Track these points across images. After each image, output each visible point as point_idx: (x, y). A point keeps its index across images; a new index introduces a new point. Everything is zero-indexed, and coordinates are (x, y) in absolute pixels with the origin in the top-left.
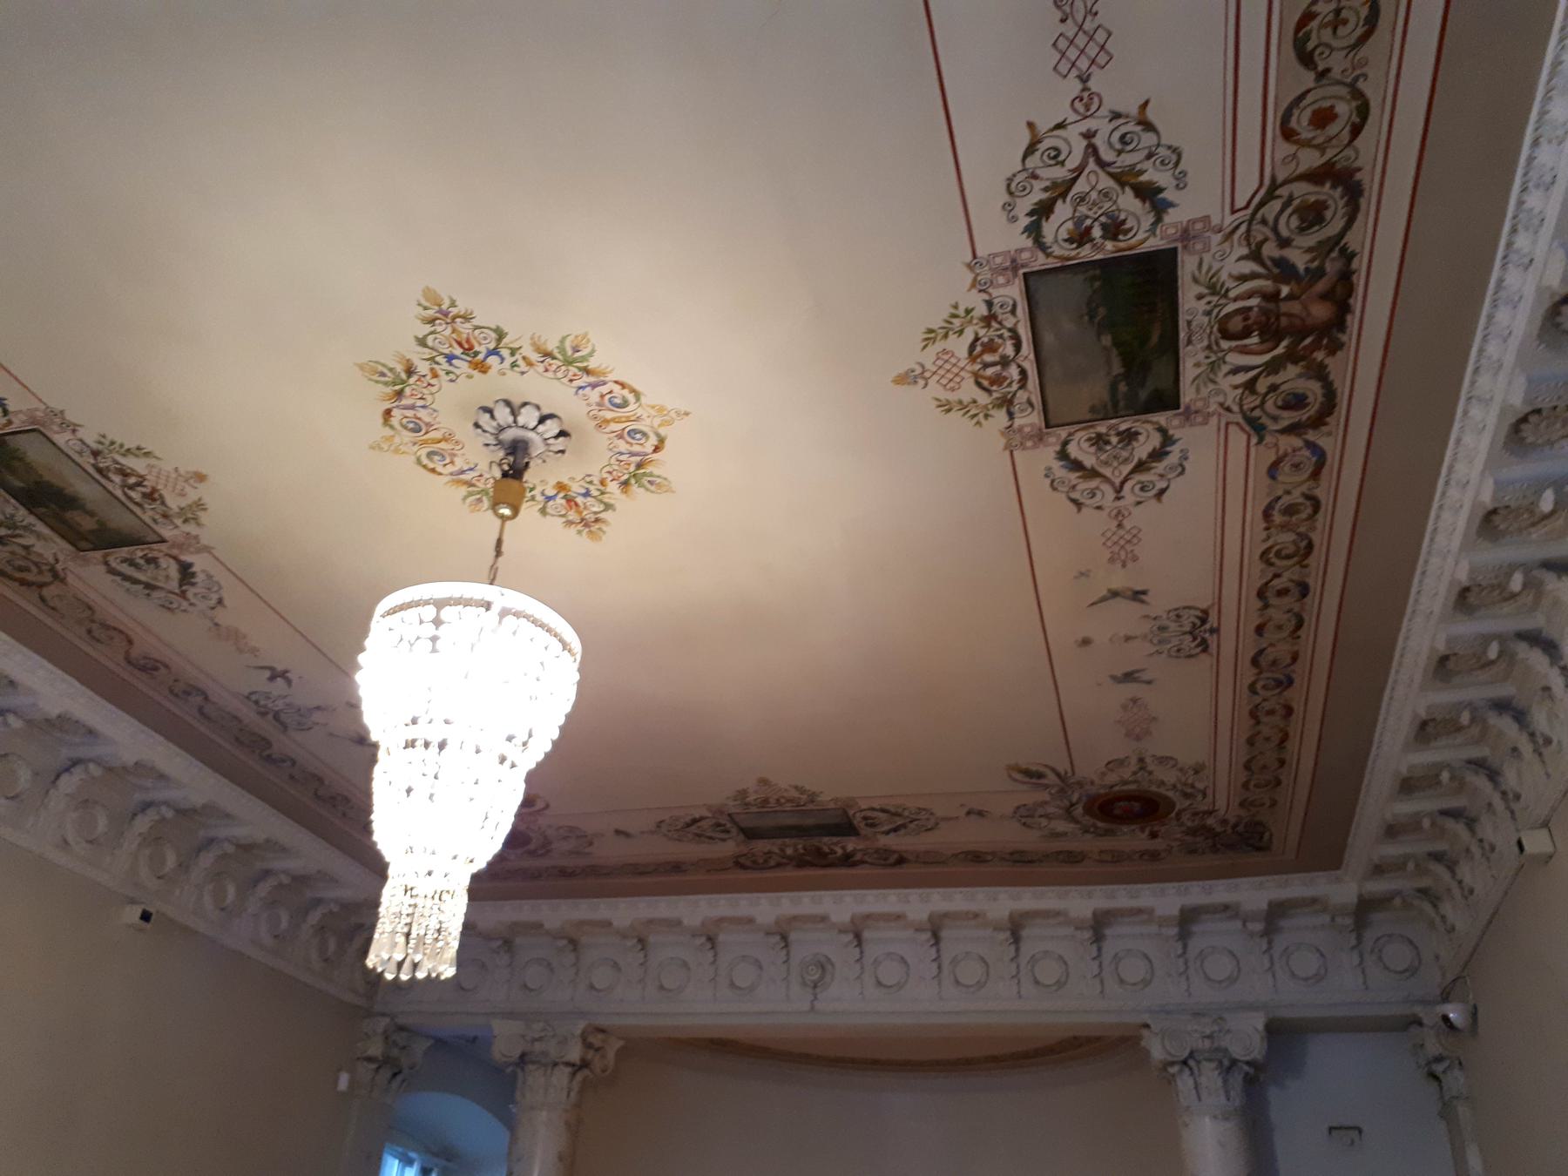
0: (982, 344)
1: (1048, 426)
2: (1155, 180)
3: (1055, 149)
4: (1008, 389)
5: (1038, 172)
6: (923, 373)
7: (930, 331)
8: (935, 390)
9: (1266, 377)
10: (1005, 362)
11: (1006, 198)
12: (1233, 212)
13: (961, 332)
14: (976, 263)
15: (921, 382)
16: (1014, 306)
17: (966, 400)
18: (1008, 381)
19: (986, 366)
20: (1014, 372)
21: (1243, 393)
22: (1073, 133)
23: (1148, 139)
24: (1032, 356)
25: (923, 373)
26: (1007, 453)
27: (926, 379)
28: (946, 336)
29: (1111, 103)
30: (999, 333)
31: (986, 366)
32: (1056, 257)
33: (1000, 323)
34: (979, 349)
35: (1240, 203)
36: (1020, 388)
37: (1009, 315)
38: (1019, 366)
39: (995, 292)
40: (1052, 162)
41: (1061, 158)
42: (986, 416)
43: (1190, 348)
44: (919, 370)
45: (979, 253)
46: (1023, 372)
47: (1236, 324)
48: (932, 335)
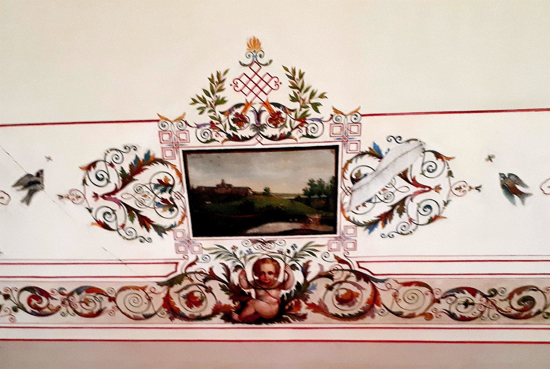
0: (279, 113)
1: (185, 153)
2: (393, 221)
3: (433, 171)
4: (228, 127)
6: (258, 64)
7: (301, 76)
8: (236, 71)
9: (220, 285)
10: (258, 128)
11: (404, 139)
12: (358, 262)
13: (294, 99)
14: (356, 116)
15: (248, 61)
16: (312, 137)
18: (237, 128)
19: (258, 115)
20: (246, 131)
21: (206, 274)
22: (443, 181)
23: (423, 220)
24: (259, 146)
25: (258, 64)
26: (158, 118)
27: (250, 66)
28: (294, 87)
29: (455, 201)
30: (288, 124)
31: (258, 115)
33: (297, 127)
34: (276, 109)
35: (361, 265)
36: (228, 135)
38: (251, 138)
39: (327, 125)
40: (425, 167)
41: (427, 173)
42: (202, 110)
43: (250, 243)
45: (363, 118)
46: (245, 139)
47: (268, 267)
48: (297, 76)
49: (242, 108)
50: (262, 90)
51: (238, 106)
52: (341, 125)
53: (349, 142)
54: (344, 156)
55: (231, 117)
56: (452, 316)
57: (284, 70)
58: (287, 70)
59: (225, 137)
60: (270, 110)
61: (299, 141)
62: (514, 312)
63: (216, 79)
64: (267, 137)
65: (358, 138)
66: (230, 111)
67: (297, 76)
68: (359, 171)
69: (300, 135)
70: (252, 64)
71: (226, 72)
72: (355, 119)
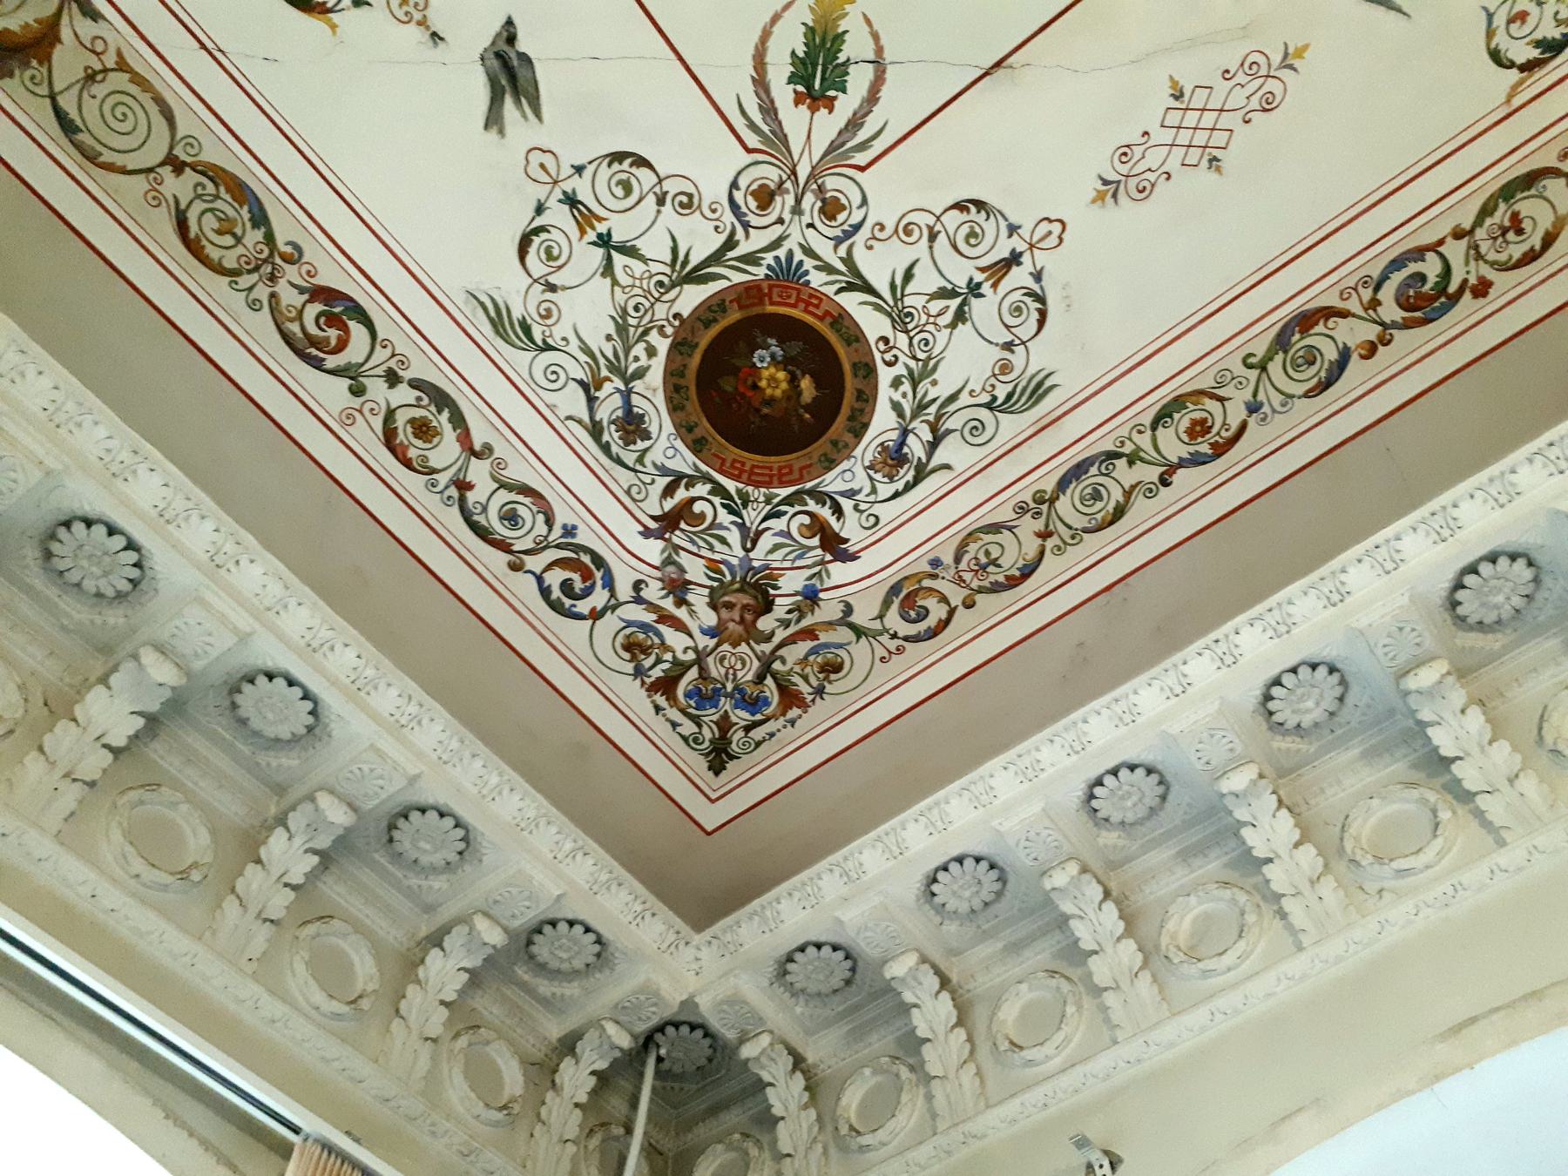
56: (182, 225)
62: (295, 328)
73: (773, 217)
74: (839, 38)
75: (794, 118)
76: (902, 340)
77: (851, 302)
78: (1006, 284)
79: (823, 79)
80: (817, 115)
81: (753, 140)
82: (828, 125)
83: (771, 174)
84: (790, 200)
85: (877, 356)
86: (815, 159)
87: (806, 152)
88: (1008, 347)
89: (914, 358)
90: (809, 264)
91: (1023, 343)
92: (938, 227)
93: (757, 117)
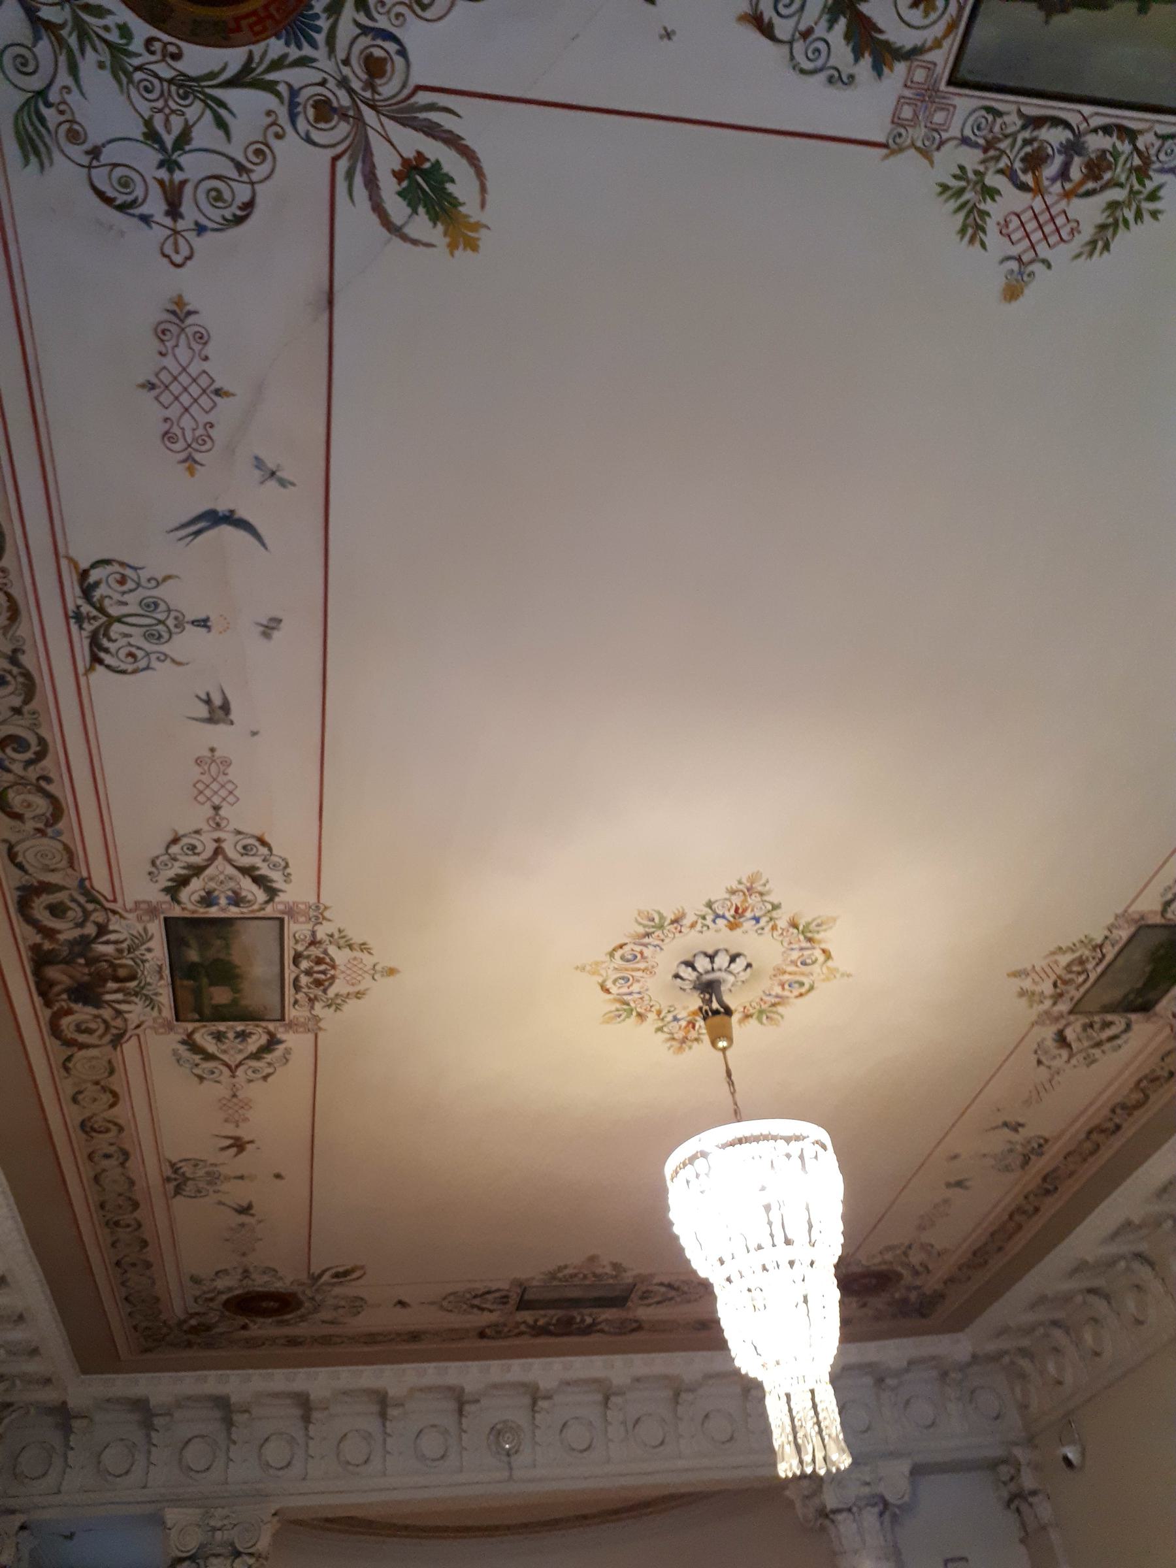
5: (802, 27)
7: (963, 231)
8: (1060, 255)
13: (991, 193)
16: (989, 109)
17: (1101, 218)
24: (1087, 110)
30: (1019, 142)
31: (1064, 174)
32: (945, 36)
33: (1006, 136)
34: (1028, 179)
37: (999, 121)
38: (1095, 131)
44: (1014, 265)
46: (1107, 130)
48: (970, 231)
49: (1082, 190)
50: (1036, 216)
51: (1089, 193)
52: (929, 125)
53: (926, 87)
54: (943, 59)
55: (1107, 176)
57: (987, 243)
58: (983, 245)
59: (1140, 144)
60: (1037, 180)
61: (1013, 108)
63: (1100, 244)
64: (1067, 125)
65: (908, 93)
66: (1103, 188)
67: (970, 231)
68: (926, 14)
69: (1006, 119)
70: (1032, 262)
71: (1078, 256)
72: (900, 135)
73: (354, 61)
74: (434, 219)
75: (411, 142)
76: (167, 73)
77: (232, 58)
78: (156, 191)
79: (419, 184)
80: (399, 160)
81: (423, 98)
82: (386, 162)
83: (388, 88)
84: (356, 85)
85: (166, 38)
86: (370, 132)
87: (380, 129)
88: (95, 153)
89: (139, 68)
90: (294, 53)
91: (90, 167)
92: (245, 178)
93: (434, 116)
